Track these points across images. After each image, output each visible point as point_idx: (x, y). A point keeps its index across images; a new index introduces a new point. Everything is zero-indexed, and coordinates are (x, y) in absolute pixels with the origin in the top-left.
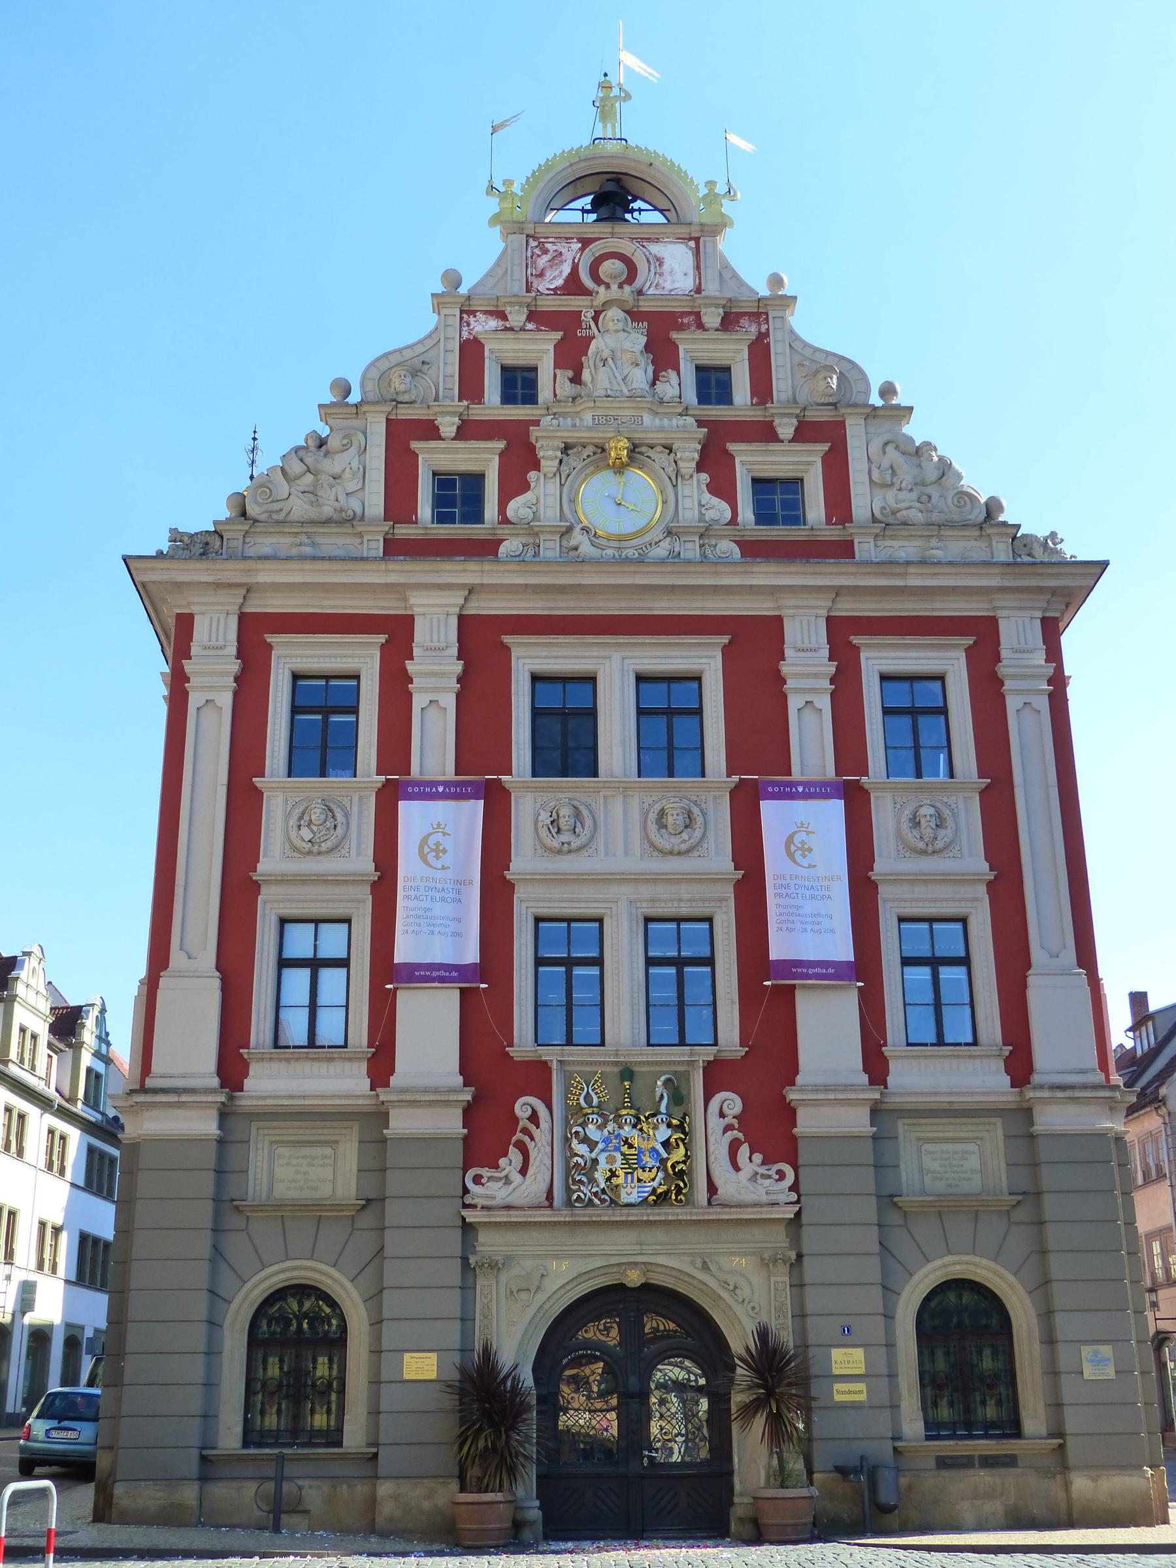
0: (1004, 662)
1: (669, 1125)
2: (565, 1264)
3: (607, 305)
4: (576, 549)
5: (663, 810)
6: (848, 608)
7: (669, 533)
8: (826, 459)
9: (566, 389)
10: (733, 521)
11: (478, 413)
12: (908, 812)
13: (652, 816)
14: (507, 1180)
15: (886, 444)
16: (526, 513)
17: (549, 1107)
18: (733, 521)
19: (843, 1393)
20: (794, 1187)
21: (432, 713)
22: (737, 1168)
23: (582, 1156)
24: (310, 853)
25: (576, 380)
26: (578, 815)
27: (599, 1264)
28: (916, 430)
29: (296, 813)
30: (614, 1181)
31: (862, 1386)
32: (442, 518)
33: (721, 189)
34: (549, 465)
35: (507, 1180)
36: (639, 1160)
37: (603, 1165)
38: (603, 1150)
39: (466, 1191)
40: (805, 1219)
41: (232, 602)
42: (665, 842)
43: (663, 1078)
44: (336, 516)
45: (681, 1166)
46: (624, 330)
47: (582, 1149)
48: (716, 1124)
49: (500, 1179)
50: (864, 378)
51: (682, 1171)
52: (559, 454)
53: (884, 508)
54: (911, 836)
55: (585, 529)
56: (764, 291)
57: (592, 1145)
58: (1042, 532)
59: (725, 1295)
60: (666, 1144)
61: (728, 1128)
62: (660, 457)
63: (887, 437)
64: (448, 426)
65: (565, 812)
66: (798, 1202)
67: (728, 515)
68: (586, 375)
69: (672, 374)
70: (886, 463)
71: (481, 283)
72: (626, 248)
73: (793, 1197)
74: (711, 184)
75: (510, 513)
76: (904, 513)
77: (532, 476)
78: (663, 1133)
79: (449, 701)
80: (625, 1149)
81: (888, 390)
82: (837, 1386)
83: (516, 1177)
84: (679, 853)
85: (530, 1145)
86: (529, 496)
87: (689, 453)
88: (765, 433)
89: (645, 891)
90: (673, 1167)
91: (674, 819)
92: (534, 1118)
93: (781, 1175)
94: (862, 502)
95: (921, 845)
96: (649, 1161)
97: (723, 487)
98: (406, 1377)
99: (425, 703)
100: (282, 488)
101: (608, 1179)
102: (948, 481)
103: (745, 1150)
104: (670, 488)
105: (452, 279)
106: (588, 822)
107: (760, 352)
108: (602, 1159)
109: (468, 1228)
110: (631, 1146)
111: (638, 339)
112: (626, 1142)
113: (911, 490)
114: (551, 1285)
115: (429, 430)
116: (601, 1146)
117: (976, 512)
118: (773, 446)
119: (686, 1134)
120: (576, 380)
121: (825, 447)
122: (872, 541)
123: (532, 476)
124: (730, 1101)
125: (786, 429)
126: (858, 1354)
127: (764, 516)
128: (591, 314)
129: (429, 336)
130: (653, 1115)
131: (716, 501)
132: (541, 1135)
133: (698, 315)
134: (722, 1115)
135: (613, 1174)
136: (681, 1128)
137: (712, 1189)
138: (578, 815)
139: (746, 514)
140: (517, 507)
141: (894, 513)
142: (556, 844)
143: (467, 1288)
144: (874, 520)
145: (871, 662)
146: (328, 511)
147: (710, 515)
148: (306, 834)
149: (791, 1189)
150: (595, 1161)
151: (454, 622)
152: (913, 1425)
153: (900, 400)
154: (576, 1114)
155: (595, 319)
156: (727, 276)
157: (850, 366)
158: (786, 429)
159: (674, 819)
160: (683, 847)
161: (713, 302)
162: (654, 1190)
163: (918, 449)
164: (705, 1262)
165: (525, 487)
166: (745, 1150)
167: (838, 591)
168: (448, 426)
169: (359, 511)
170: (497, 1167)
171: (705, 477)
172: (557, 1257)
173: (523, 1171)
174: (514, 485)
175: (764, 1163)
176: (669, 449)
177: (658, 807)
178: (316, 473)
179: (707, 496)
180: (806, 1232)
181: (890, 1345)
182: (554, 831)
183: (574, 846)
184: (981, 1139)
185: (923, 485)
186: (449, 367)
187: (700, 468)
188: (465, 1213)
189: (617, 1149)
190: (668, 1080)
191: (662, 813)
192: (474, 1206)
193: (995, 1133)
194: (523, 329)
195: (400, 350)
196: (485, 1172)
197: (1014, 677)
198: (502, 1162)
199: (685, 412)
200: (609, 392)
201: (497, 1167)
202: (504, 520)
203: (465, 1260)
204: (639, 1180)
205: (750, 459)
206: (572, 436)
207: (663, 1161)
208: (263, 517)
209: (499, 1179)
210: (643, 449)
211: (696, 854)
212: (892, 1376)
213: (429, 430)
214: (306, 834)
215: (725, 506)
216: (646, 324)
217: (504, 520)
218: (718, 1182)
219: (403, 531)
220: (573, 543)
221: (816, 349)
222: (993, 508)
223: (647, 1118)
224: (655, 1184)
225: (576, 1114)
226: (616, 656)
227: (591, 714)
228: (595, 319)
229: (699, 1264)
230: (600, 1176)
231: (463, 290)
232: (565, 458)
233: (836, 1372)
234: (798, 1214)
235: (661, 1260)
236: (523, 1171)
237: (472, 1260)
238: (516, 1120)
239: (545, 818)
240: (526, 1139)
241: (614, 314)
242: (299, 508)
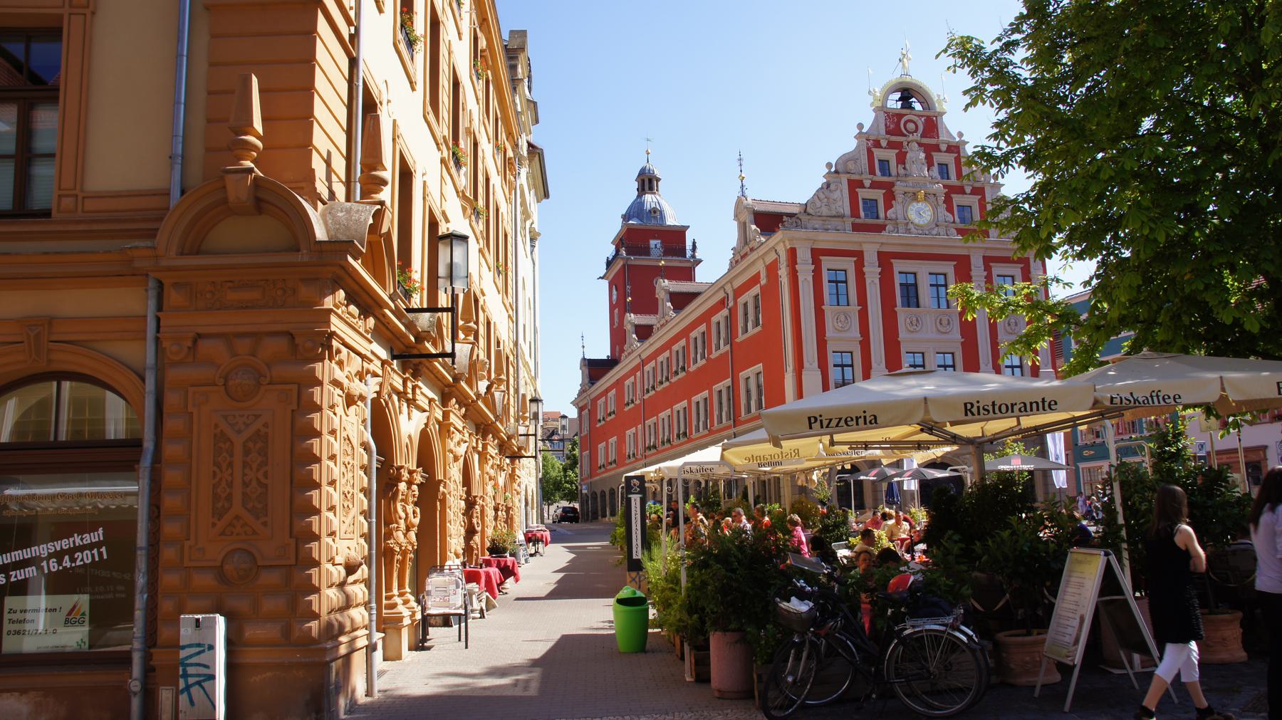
3: (912, 141)
6: (988, 254)
8: (980, 201)
9: (902, 171)
10: (954, 222)
11: (875, 179)
13: (938, 321)
16: (894, 216)
18: (954, 222)
25: (904, 168)
26: (917, 320)
32: (866, 216)
33: (942, 98)
41: (809, 245)
54: (1008, 328)
56: (958, 139)
62: (932, 198)
64: (867, 183)
65: (914, 319)
68: (907, 166)
72: (915, 118)
74: (939, 96)
77: (893, 202)
79: (877, 281)
88: (961, 190)
91: (945, 322)
97: (950, 209)
100: (818, 204)
105: (860, 126)
111: (922, 155)
115: (862, 186)
120: (904, 168)
121: (980, 197)
123: (893, 202)
125: (968, 190)
127: (963, 220)
139: (957, 219)
140: (889, 212)
146: (834, 213)
151: (876, 254)
158: (968, 190)
159: (945, 322)
161: (944, 142)
165: (891, 206)
167: (987, 249)
168: (867, 183)
171: (945, 206)
174: (888, 206)
178: (828, 199)
187: (944, 202)
191: (941, 320)
194: (885, 148)
202: (886, 217)
206: (907, 190)
213: (861, 185)
217: (886, 217)
219: (857, 221)
227: (915, 285)
231: (864, 130)
242: (825, 211)
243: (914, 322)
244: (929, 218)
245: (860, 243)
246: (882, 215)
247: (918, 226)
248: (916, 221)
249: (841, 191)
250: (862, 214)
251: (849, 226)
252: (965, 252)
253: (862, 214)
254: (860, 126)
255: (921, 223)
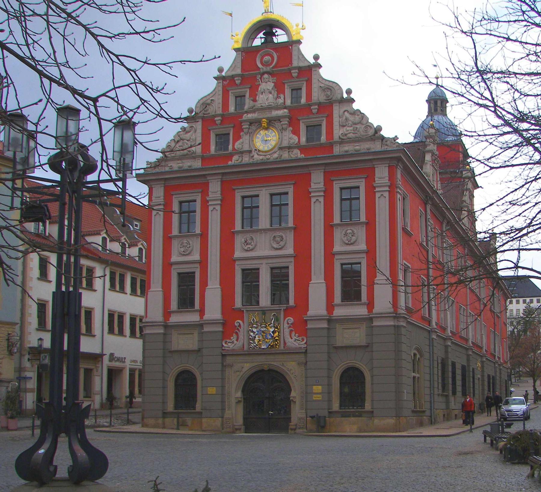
0: (376, 182)
1: (274, 327)
2: (248, 364)
4: (253, 156)
5: (275, 236)
7: (281, 148)
12: (344, 232)
14: (233, 342)
15: (345, 111)
16: (241, 146)
17: (243, 322)
19: (316, 397)
20: (306, 343)
21: (214, 211)
22: (292, 338)
23: (251, 336)
24: (184, 255)
25: (255, 100)
27: (256, 364)
28: (355, 106)
29: (180, 243)
30: (260, 343)
31: (321, 396)
34: (246, 130)
35: (233, 342)
36: (266, 336)
37: (257, 338)
38: (257, 334)
39: (223, 346)
40: (308, 351)
42: (275, 246)
43: (273, 314)
44: (189, 153)
45: (276, 338)
46: (269, 81)
47: (252, 334)
48: (286, 325)
49: (231, 342)
50: (340, 88)
51: (277, 339)
52: (248, 126)
53: (342, 134)
55: (256, 150)
57: (254, 332)
58: (392, 136)
59: (288, 372)
60: (274, 332)
61: (290, 327)
63: (345, 109)
66: (306, 347)
67: (297, 140)
69: (282, 96)
70: (344, 118)
71: (229, 70)
73: (305, 346)
75: (236, 147)
76: (348, 135)
77: (242, 134)
78: (272, 330)
80: (262, 334)
81: (349, 92)
82: (315, 396)
83: (235, 342)
84: (280, 249)
85: (239, 333)
86: (241, 140)
87: (285, 122)
89: (270, 261)
90: (275, 338)
92: (240, 326)
93: (303, 340)
94: (337, 132)
95: (347, 242)
96: (269, 337)
97: (296, 132)
98: (209, 393)
99: (212, 209)
101: (258, 342)
102: (364, 122)
103: (293, 333)
104: (281, 134)
106: (255, 241)
107: (309, 83)
108: (257, 336)
109: (223, 356)
110: (264, 333)
111: (270, 86)
112: (263, 332)
113: (351, 126)
114: (244, 370)
116: (256, 333)
117: (371, 131)
118: (311, 116)
119: (278, 329)
122: (339, 145)
124: (291, 320)
126: (320, 387)
127: (308, 140)
128: (260, 76)
129: (214, 90)
130: (270, 324)
131: (294, 136)
132: (241, 330)
133: (290, 73)
134: (288, 324)
135: (260, 340)
136: (277, 328)
137: (285, 343)
138: (252, 239)
139: (303, 140)
140: (237, 145)
141: (346, 135)
142: (246, 248)
143: (223, 371)
144: (340, 138)
145: (336, 185)
147: (292, 141)
148: (182, 249)
149: (305, 343)
150: (255, 337)
152: (336, 406)
153: (352, 96)
154: (251, 324)
155: (261, 78)
156: (300, 57)
157: (336, 85)
160: (280, 247)
162: (270, 345)
163: (354, 112)
164: (283, 364)
165: (239, 138)
166: (293, 333)
169: (194, 151)
170: (230, 339)
171: (291, 128)
172: (246, 363)
173: (237, 340)
174: (237, 138)
175: (298, 337)
176: (280, 120)
177: (274, 235)
178: (183, 140)
179: (291, 135)
180: (309, 355)
181: (329, 385)
182: (245, 244)
183: (251, 248)
184: (360, 328)
185: (355, 124)
186: (219, 99)
188: (222, 351)
189: (260, 333)
190: (274, 315)
191: (275, 237)
192: (225, 350)
193: (364, 327)
195: (206, 97)
196: (228, 341)
197: (378, 187)
198: (232, 338)
199: (285, 108)
200: (262, 105)
201: (230, 339)
203: (222, 363)
204: (266, 342)
205: (306, 121)
207: (272, 337)
208: (169, 156)
209: (231, 342)
210: (273, 122)
211: (284, 248)
212: (329, 393)
214: (182, 249)
215: (296, 138)
216: (276, 78)
217: (234, 149)
218: (287, 342)
220: (252, 155)
221: (326, 80)
222: (379, 129)
223: (269, 325)
224: (270, 343)
225: (251, 324)
226: (264, 189)
228: (261, 78)
229: (281, 364)
230: (256, 341)
232: (251, 127)
233: (314, 392)
234: (306, 350)
235: (272, 363)
236: (237, 340)
237: (224, 364)
238: (236, 326)
239: (243, 240)
240: (237, 331)
241: (266, 76)
243: (249, 241)
244: (273, 143)
245: (204, 176)
246: (230, 147)
247: (263, 152)
248: (261, 148)
249: (195, 131)
250: (213, 148)
251: (197, 164)
252: (305, 171)
253: (213, 148)
254: (221, 70)
255: (266, 149)
